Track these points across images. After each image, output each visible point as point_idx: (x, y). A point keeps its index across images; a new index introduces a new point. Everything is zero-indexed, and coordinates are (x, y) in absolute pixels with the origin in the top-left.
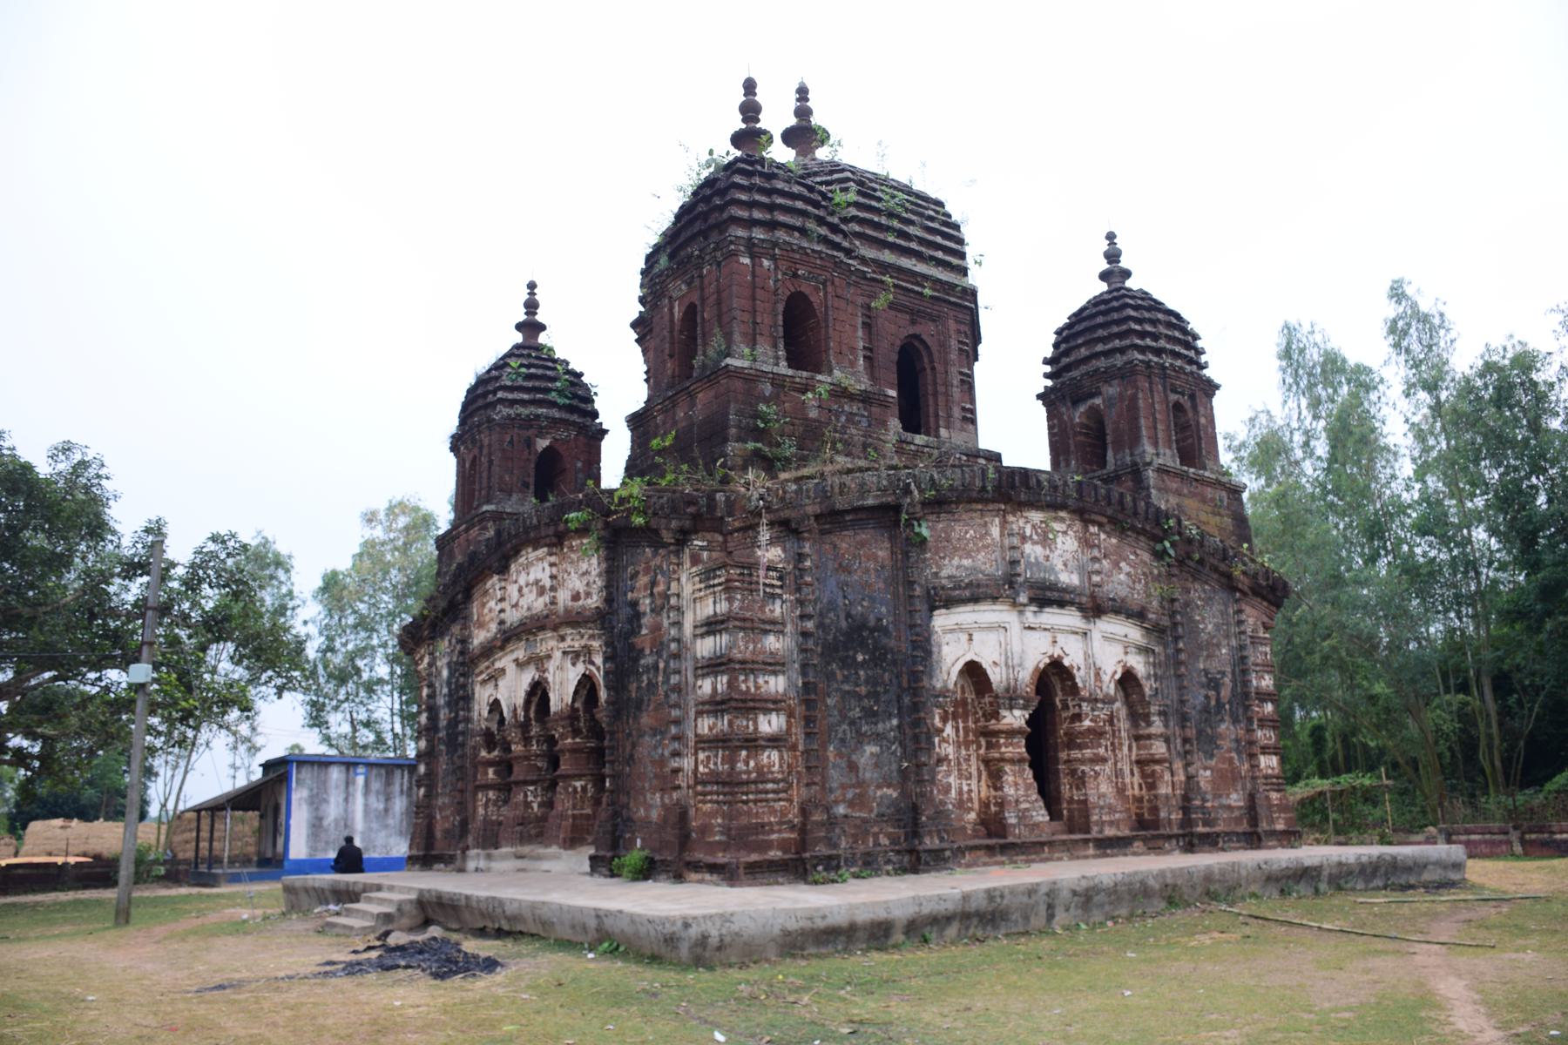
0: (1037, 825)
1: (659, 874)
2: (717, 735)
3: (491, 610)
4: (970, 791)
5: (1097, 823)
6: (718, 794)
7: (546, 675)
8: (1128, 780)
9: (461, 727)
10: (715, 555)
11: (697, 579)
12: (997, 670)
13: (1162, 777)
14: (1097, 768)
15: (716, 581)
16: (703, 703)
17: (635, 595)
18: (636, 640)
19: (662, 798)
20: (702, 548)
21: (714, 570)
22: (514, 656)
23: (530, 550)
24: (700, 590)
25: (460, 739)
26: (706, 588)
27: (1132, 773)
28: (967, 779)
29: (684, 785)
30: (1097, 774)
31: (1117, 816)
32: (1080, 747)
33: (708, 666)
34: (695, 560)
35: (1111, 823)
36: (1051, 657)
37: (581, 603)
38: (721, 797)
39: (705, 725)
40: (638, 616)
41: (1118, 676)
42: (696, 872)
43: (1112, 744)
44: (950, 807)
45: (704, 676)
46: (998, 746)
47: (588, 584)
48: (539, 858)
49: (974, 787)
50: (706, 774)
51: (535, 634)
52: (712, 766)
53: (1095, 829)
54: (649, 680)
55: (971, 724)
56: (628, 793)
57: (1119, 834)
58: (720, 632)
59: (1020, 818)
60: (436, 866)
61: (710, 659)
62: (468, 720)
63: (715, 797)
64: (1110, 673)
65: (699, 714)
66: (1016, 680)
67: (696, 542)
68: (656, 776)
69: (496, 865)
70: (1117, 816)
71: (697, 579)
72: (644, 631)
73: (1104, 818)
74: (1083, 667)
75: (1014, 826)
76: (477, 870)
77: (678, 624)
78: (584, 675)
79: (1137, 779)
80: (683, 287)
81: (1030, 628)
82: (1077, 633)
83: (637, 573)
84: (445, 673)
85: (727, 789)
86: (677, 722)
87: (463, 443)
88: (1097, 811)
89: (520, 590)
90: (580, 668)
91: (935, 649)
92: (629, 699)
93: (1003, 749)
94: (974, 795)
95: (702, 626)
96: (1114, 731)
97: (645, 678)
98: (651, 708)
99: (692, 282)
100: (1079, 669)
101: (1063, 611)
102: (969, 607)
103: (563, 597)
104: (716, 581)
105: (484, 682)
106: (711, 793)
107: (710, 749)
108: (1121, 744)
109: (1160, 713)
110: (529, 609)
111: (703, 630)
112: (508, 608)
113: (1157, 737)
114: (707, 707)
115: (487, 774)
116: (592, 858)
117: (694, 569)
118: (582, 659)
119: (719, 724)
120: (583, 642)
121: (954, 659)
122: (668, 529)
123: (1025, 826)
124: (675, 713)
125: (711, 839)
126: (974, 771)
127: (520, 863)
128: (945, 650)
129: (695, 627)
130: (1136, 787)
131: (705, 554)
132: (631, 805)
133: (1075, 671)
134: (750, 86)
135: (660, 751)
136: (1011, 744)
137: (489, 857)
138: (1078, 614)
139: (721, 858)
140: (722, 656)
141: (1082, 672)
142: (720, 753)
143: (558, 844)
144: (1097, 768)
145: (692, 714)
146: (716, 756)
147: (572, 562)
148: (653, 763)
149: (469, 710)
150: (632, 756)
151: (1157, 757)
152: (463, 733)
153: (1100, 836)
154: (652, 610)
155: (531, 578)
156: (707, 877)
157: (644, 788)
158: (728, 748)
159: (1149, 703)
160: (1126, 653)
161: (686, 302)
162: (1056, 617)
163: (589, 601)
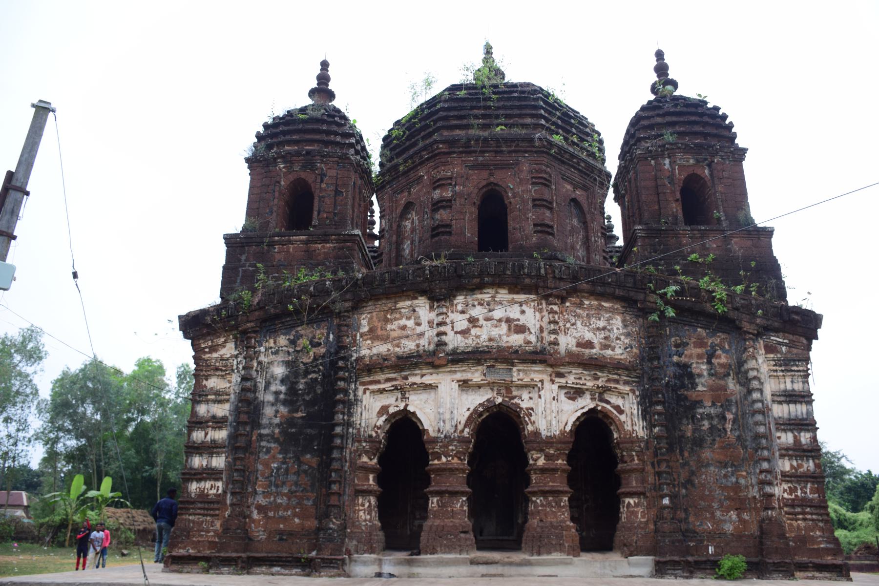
1: (770, 573)
2: (804, 473)
3: (404, 328)
6: (812, 514)
7: (516, 401)
9: (338, 430)
10: (795, 351)
11: (773, 363)
15: (795, 368)
16: (787, 449)
17: (683, 359)
18: (692, 395)
19: (738, 515)
20: (780, 343)
21: (794, 360)
22: (459, 376)
23: (503, 291)
24: (776, 371)
25: (338, 441)
26: (782, 371)
29: (777, 506)
33: (789, 424)
34: (769, 349)
37: (594, 351)
38: (814, 517)
39: (786, 465)
40: (686, 374)
42: (800, 571)
45: (785, 431)
47: (606, 338)
48: (528, 563)
50: (793, 500)
51: (513, 365)
52: (799, 493)
54: (712, 428)
56: (686, 510)
58: (801, 403)
60: (258, 569)
61: (790, 420)
62: (349, 424)
63: (809, 517)
65: (782, 456)
67: (772, 338)
68: (728, 498)
69: (416, 570)
71: (773, 363)
72: (700, 388)
76: (379, 575)
77: (761, 391)
78: (593, 411)
80: (692, 161)
83: (688, 344)
84: (279, 371)
85: (818, 511)
86: (768, 460)
87: (284, 162)
89: (473, 321)
90: (586, 403)
92: (682, 436)
95: (779, 396)
97: (706, 424)
98: (716, 446)
99: (703, 162)
103: (567, 342)
104: (795, 368)
105: (382, 391)
106: (804, 513)
107: (798, 482)
110: (490, 340)
111: (782, 399)
112: (451, 334)
114: (791, 452)
115: (369, 480)
116: (657, 563)
117: (772, 356)
118: (588, 396)
119: (805, 466)
120: (600, 383)
122: (751, 323)
124: (766, 453)
125: (816, 547)
127: (482, 569)
129: (772, 395)
131: (784, 349)
132: (691, 519)
134: (660, 55)
135: (734, 480)
137: (409, 563)
139: (829, 559)
140: (803, 419)
142: (809, 485)
143: (561, 551)
145: (777, 454)
146: (806, 487)
147: (577, 316)
148: (724, 488)
149: (350, 415)
150: (689, 482)
152: (342, 437)
154: (710, 375)
155: (498, 313)
156: (817, 574)
157: (711, 507)
158: (818, 483)
161: (690, 171)
163: (609, 352)
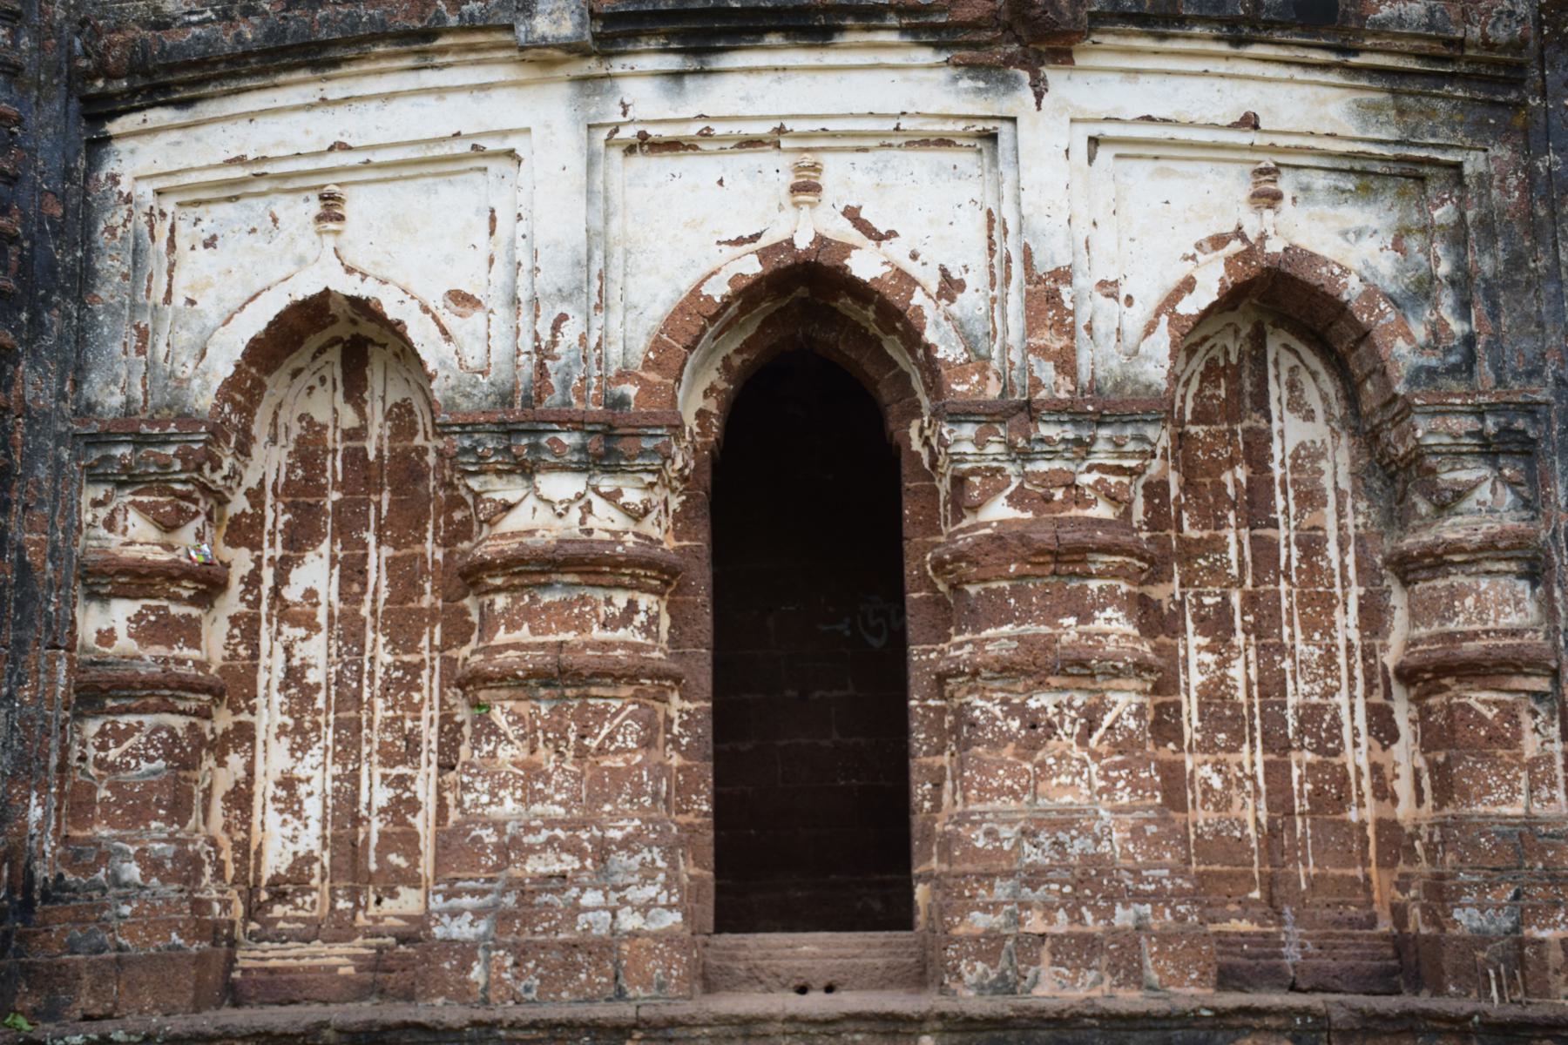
0: (603, 949)
4: (403, 807)
5: (987, 948)
8: (1357, 757)
12: (467, 327)
13: (1504, 737)
14: (1043, 701)
27: (1383, 727)
28: (388, 758)
30: (1038, 729)
31: (1124, 917)
32: (977, 617)
35: (1078, 950)
36: (764, 255)
41: (1191, 306)
43: (1251, 600)
44: (132, 872)
46: (488, 623)
49: (424, 787)
53: (974, 971)
55: (432, 550)
57: (1130, 999)
59: (504, 919)
64: (1148, 289)
66: (543, 354)
70: (1124, 917)
73: (1035, 923)
74: (975, 280)
75: (466, 952)
79: (1405, 755)
81: (646, 145)
82: (944, 142)
88: (1002, 889)
91: (111, 265)
93: (501, 637)
94: (423, 823)
96: (1265, 553)
100: (950, 287)
101: (831, 58)
102: (298, 90)
108: (1319, 606)
109: (1489, 450)
113: (1490, 547)
121: (238, 295)
123: (521, 953)
126: (430, 735)
128: (195, 267)
130: (1403, 787)
133: (918, 298)
136: (529, 614)
138: (926, 56)
141: (970, 303)
144: (1043, 701)
151: (1471, 648)
153: (1000, 1005)
159: (1408, 408)
160: (1272, 199)
162: (803, 79)
